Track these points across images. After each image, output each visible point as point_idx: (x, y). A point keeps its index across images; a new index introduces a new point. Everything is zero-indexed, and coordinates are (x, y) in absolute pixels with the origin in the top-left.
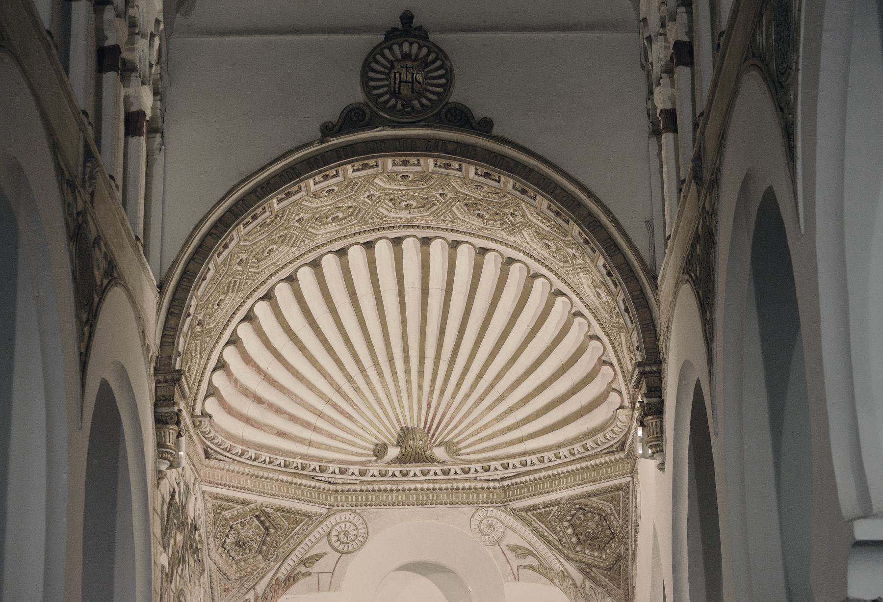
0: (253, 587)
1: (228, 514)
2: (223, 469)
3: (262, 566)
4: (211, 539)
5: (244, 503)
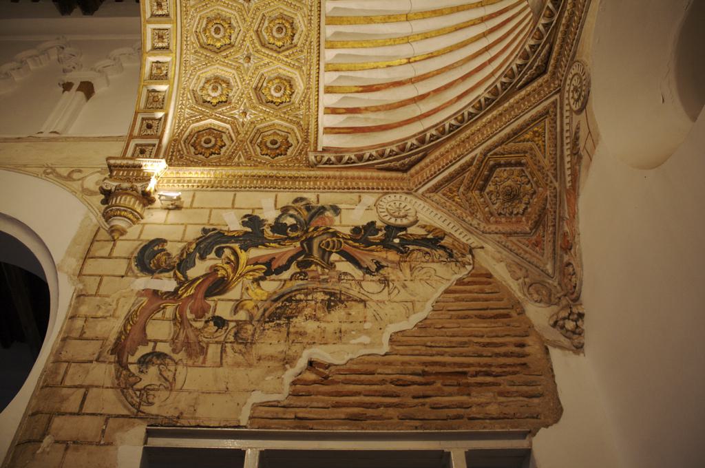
0: (562, 219)
1: (461, 189)
2: (427, 166)
3: (548, 193)
4: (469, 218)
5: (463, 169)
